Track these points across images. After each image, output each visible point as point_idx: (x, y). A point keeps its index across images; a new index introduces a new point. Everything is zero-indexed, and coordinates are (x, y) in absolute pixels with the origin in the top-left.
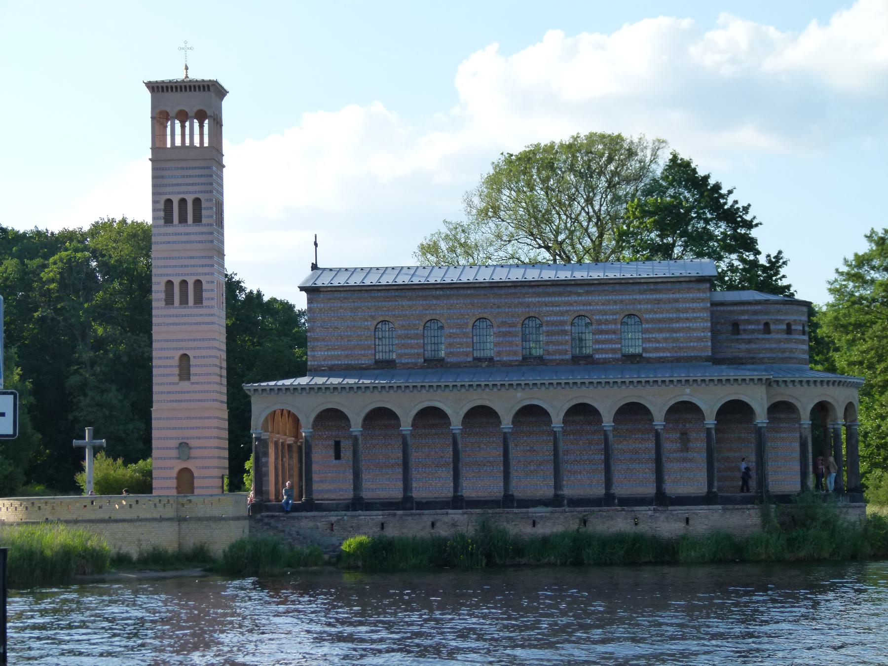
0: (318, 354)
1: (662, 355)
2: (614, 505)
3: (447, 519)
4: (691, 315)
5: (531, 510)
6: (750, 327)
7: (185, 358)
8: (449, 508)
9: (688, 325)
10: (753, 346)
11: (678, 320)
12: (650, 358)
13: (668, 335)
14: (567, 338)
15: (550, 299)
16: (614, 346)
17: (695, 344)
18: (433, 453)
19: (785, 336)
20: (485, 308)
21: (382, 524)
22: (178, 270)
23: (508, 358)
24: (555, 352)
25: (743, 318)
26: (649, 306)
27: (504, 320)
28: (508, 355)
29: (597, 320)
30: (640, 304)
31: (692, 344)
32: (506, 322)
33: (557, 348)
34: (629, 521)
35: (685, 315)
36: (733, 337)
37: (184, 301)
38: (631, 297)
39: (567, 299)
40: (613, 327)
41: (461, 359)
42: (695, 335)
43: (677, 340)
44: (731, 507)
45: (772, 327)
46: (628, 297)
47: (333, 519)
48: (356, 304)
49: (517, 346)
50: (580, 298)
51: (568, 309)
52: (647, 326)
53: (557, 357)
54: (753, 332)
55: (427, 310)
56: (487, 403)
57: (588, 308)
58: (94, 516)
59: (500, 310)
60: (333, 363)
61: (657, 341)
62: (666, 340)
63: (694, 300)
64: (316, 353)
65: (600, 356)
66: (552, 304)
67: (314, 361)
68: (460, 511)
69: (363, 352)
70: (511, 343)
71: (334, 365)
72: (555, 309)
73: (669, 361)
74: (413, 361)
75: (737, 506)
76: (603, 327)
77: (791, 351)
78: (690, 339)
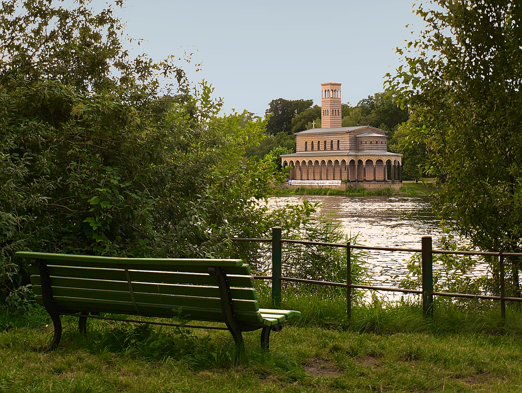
11: (345, 141)
43: (344, 146)
63: (347, 137)
78: (346, 146)
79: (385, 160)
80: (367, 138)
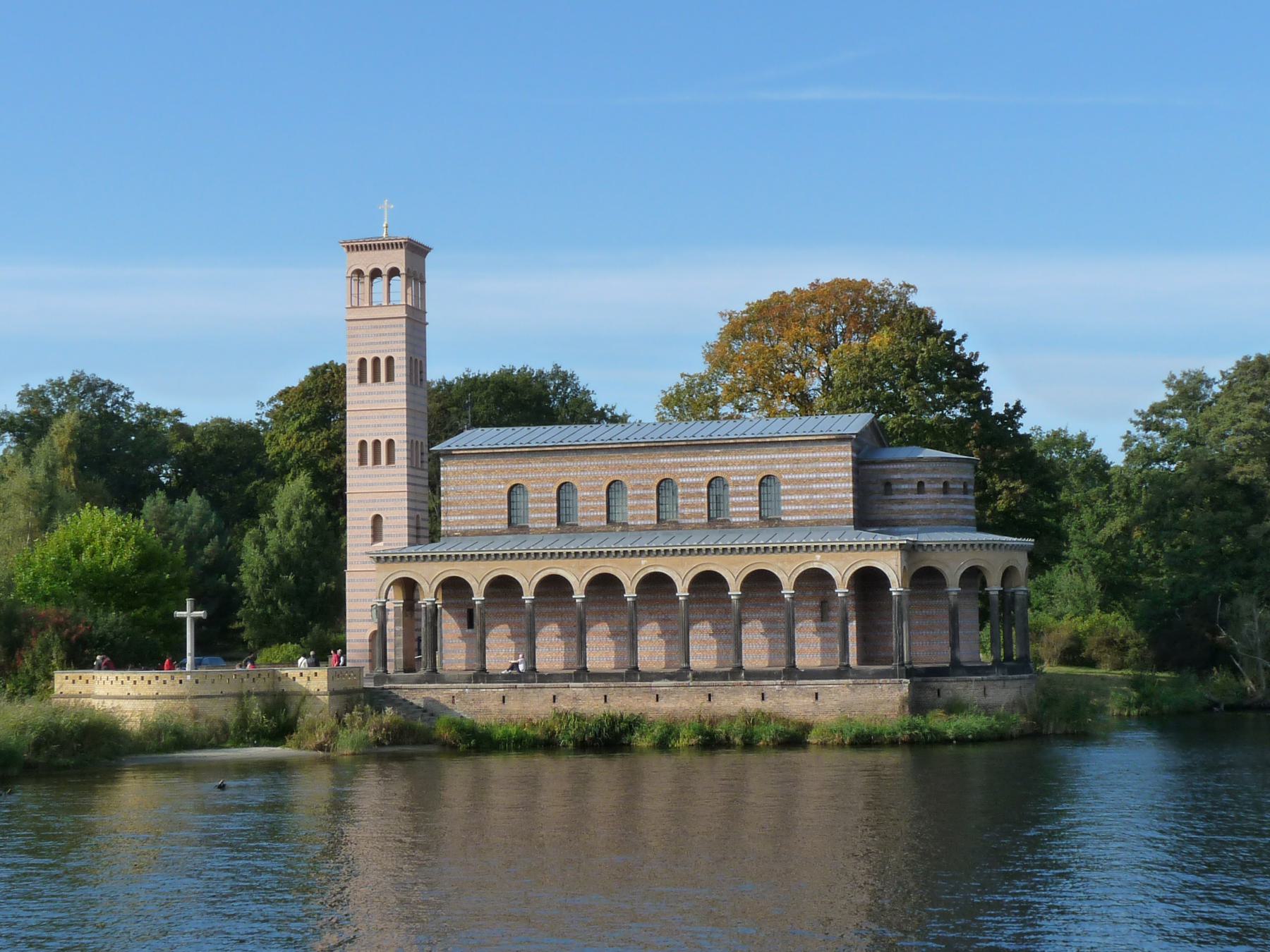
0: (451, 519)
1: (801, 518)
2: (741, 679)
3: (569, 692)
4: (832, 475)
5: (654, 683)
6: (903, 487)
7: (377, 519)
8: (571, 681)
9: (828, 486)
10: (906, 507)
11: (819, 480)
12: (788, 521)
13: (807, 497)
14: (703, 500)
15: (685, 460)
16: (751, 509)
17: (836, 506)
18: (566, 622)
19: (942, 496)
20: (619, 470)
21: (504, 697)
22: (371, 430)
23: (643, 522)
24: (691, 516)
25: (895, 477)
26: (788, 466)
27: (638, 482)
28: (643, 519)
29: (734, 482)
30: (779, 464)
31: (833, 506)
32: (640, 484)
33: (693, 511)
34: (755, 696)
35: (825, 475)
36: (885, 497)
37: (377, 461)
38: (769, 456)
39: (703, 459)
40: (751, 488)
41: (595, 523)
42: (836, 496)
43: (817, 502)
44: (862, 681)
45: (927, 486)
46: (766, 457)
47: (455, 691)
48: (489, 467)
49: (652, 509)
50: (716, 458)
51: (704, 469)
52: (786, 487)
53: (693, 521)
54: (905, 492)
55: (561, 472)
56: (611, 571)
57: (725, 468)
58: (173, 693)
59: (634, 471)
60: (466, 528)
61: (796, 503)
62: (805, 502)
63: (835, 459)
64: (449, 518)
65: (737, 520)
66: (689, 465)
67: (448, 526)
68: (581, 684)
69: (496, 517)
70: (645, 507)
71: (467, 531)
72: (690, 469)
73: (808, 525)
74: (546, 525)
75: (868, 681)
76: (740, 489)
77: (949, 511)
78: (831, 501)
79: (841, 570)
80: (927, 467)
